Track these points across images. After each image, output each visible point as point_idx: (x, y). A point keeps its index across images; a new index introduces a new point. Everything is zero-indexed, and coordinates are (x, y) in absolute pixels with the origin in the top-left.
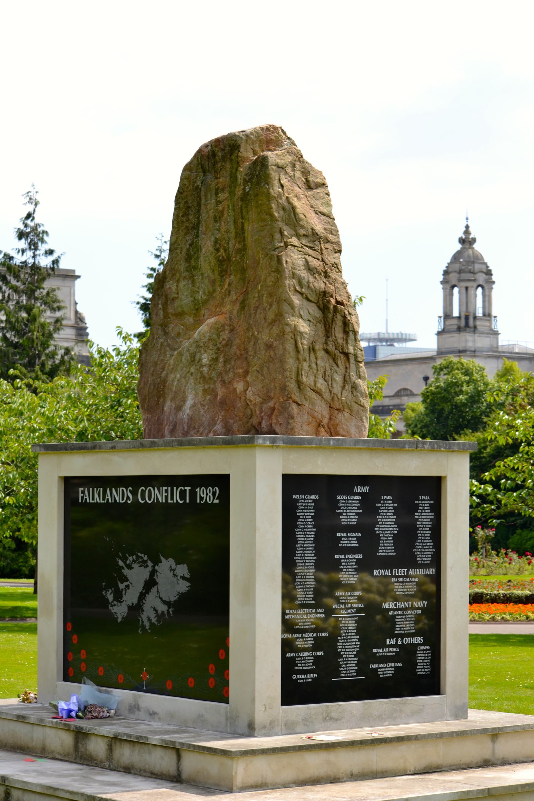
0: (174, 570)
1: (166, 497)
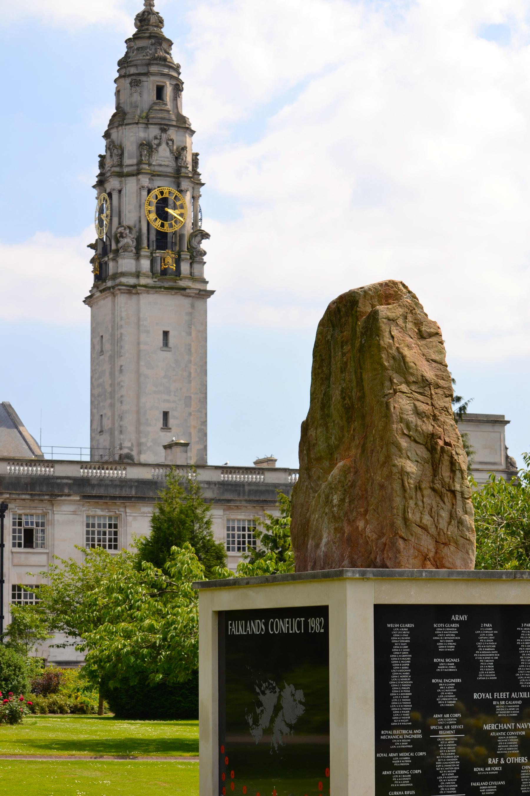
0: (293, 695)
1: (288, 627)
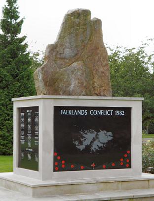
1: (103, 113)
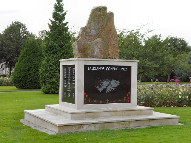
1: (114, 69)
